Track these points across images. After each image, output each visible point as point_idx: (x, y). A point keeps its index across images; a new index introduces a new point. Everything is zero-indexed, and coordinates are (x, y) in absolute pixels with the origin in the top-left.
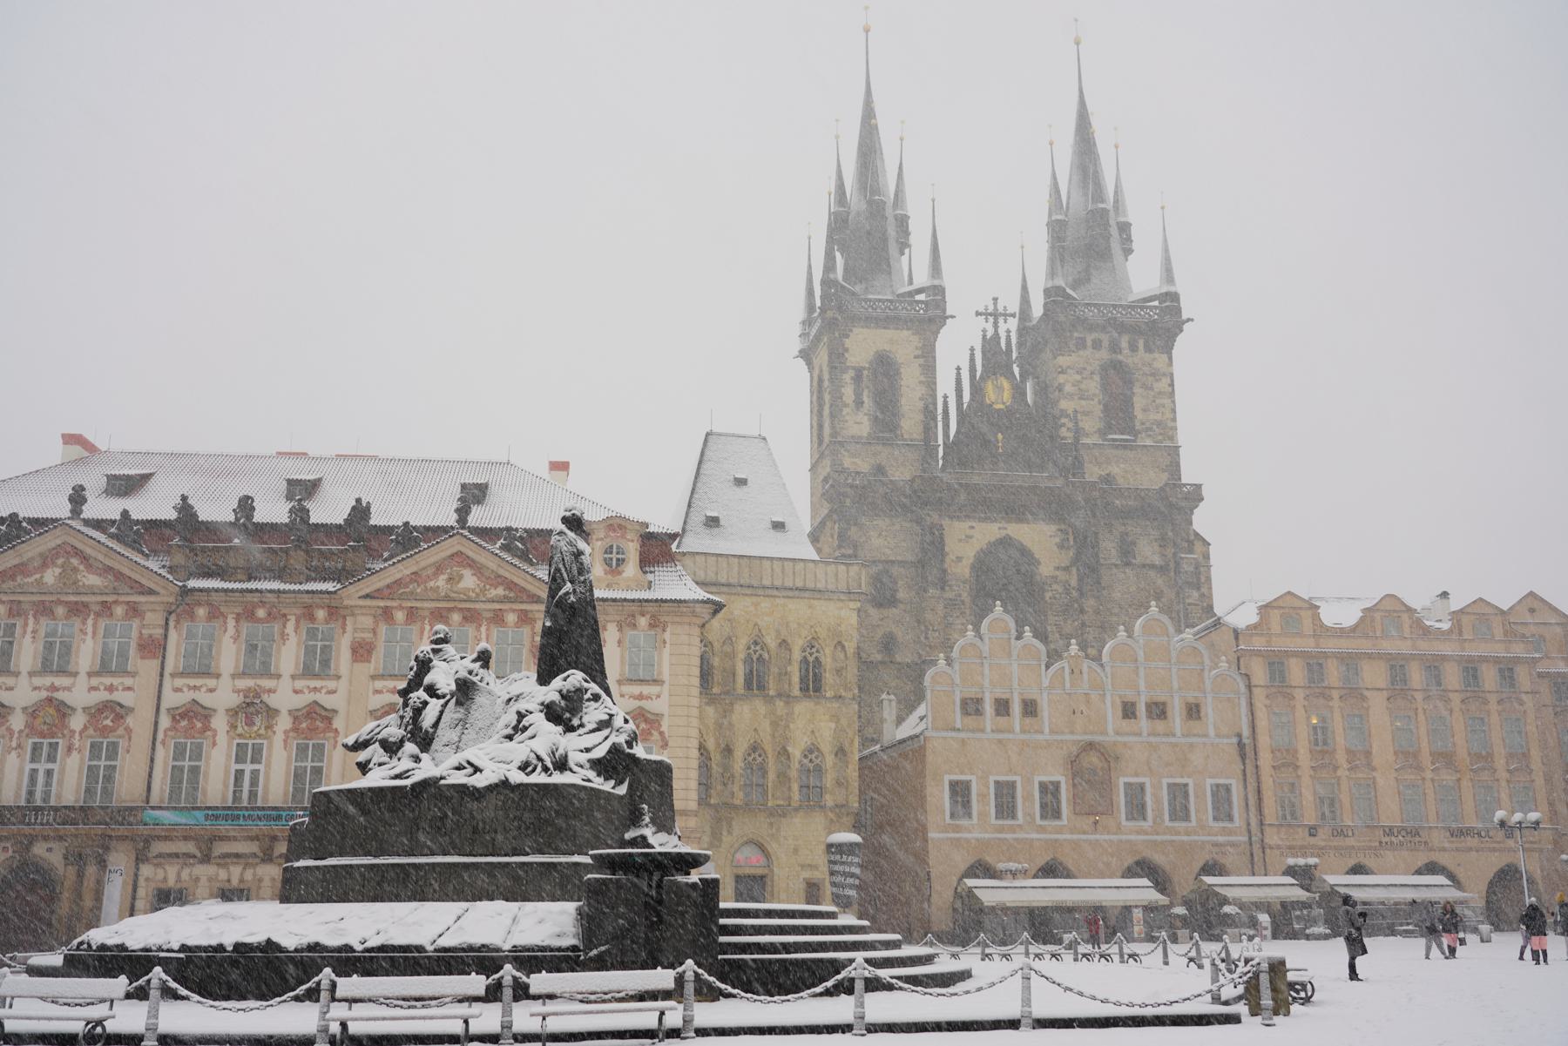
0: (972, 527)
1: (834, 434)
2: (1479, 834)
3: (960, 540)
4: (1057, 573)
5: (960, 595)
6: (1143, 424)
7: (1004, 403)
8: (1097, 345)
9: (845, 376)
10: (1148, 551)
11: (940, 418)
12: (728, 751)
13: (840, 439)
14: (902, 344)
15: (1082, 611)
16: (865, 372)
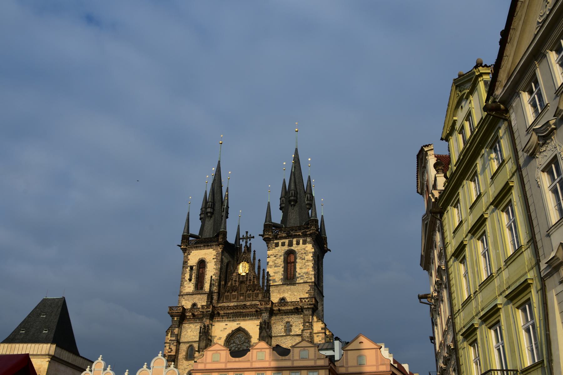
0: (226, 325)
3: (221, 331)
6: (299, 274)
7: (245, 273)
8: (283, 244)
10: (297, 328)
13: (182, 294)
16: (194, 267)
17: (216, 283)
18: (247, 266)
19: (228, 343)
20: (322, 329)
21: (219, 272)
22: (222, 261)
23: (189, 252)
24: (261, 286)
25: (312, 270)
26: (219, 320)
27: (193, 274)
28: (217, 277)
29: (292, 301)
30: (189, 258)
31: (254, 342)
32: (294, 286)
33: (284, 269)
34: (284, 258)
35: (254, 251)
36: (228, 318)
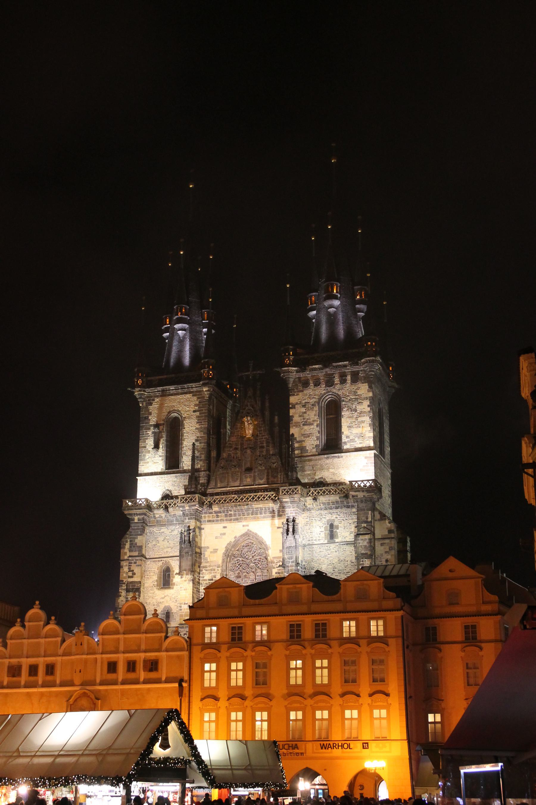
0: (225, 527)
2: (342, 746)
3: (216, 538)
6: (347, 437)
8: (317, 384)
17: (201, 454)
19: (229, 558)
20: (390, 531)
21: (206, 435)
22: (210, 415)
23: (149, 400)
25: (370, 429)
26: (211, 519)
28: (203, 444)
30: (150, 411)
34: (320, 408)
36: (226, 516)
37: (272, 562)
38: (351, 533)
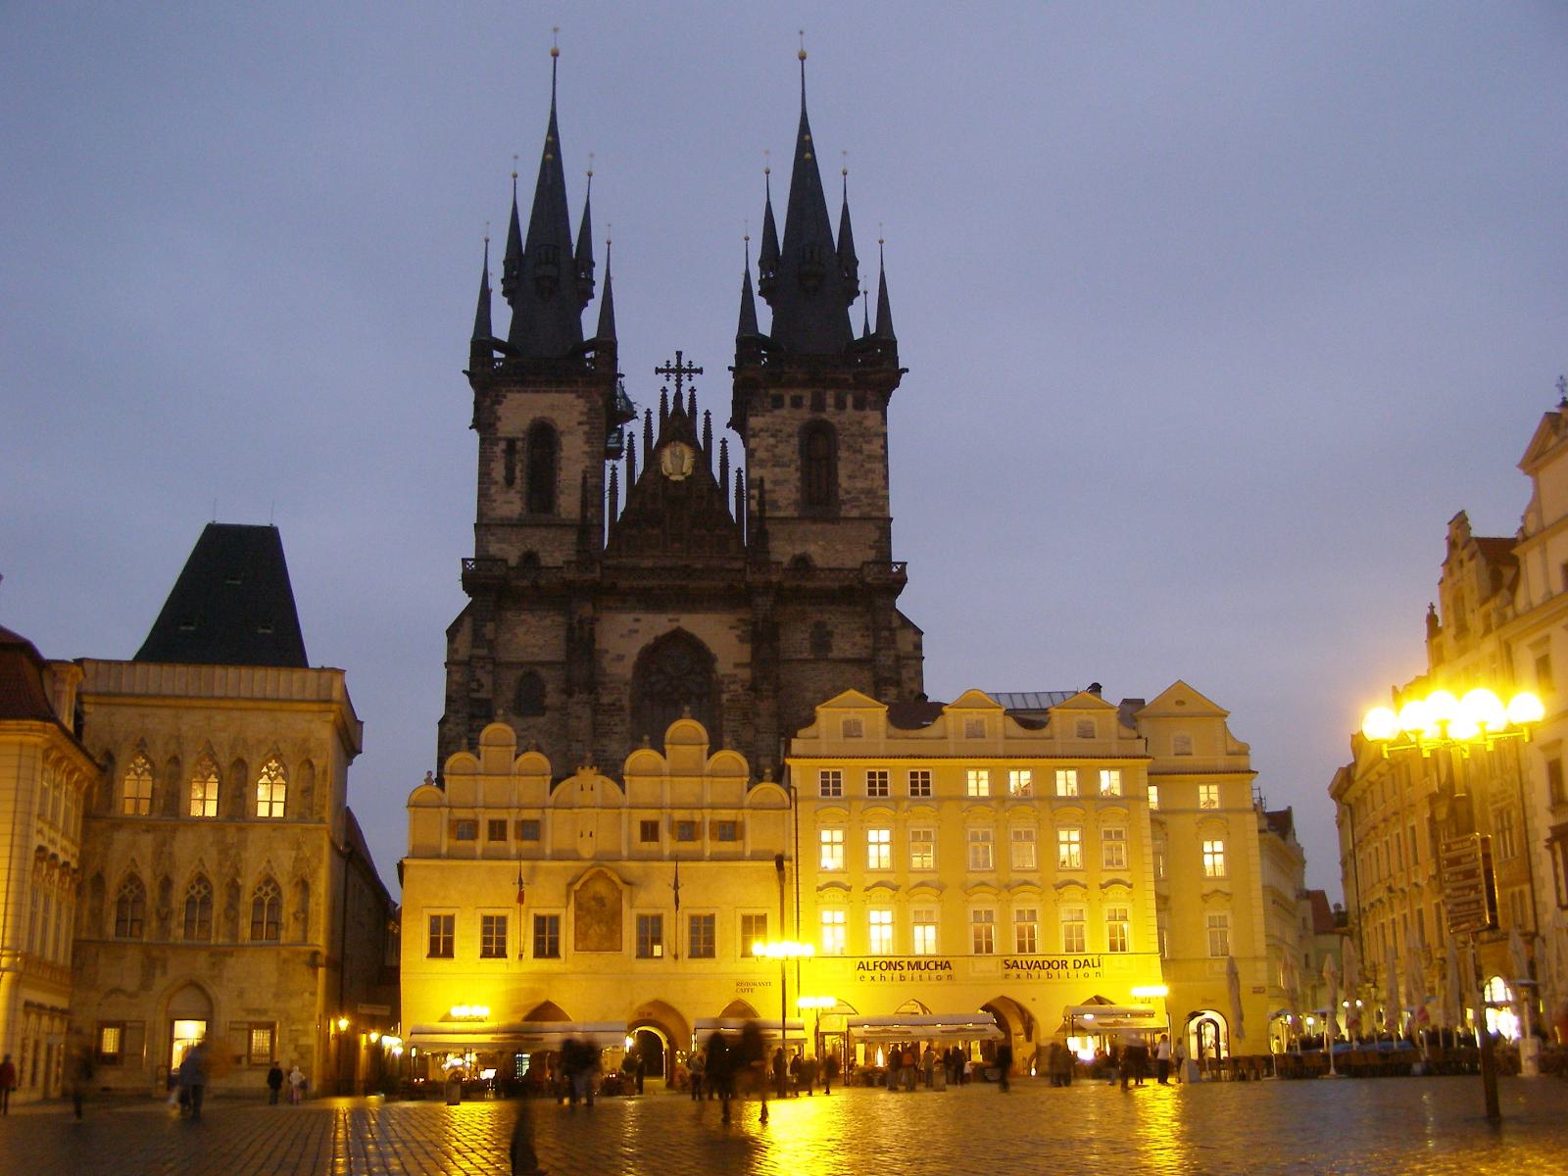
0: (637, 620)
1: (480, 515)
3: (622, 636)
4: (736, 671)
5: (620, 700)
6: (848, 492)
7: (683, 474)
8: (797, 403)
9: (495, 449)
10: (848, 641)
11: (607, 494)
12: (167, 884)
13: (485, 521)
14: (565, 409)
15: (757, 715)
16: (519, 444)
18: (686, 457)
23: (497, 396)
24: (734, 518)
27: (516, 465)
29: (833, 565)
30: (499, 414)
31: (722, 672)
32: (833, 523)
33: (802, 472)
34: (801, 445)
35: (707, 413)
37: (722, 682)
38: (854, 644)
